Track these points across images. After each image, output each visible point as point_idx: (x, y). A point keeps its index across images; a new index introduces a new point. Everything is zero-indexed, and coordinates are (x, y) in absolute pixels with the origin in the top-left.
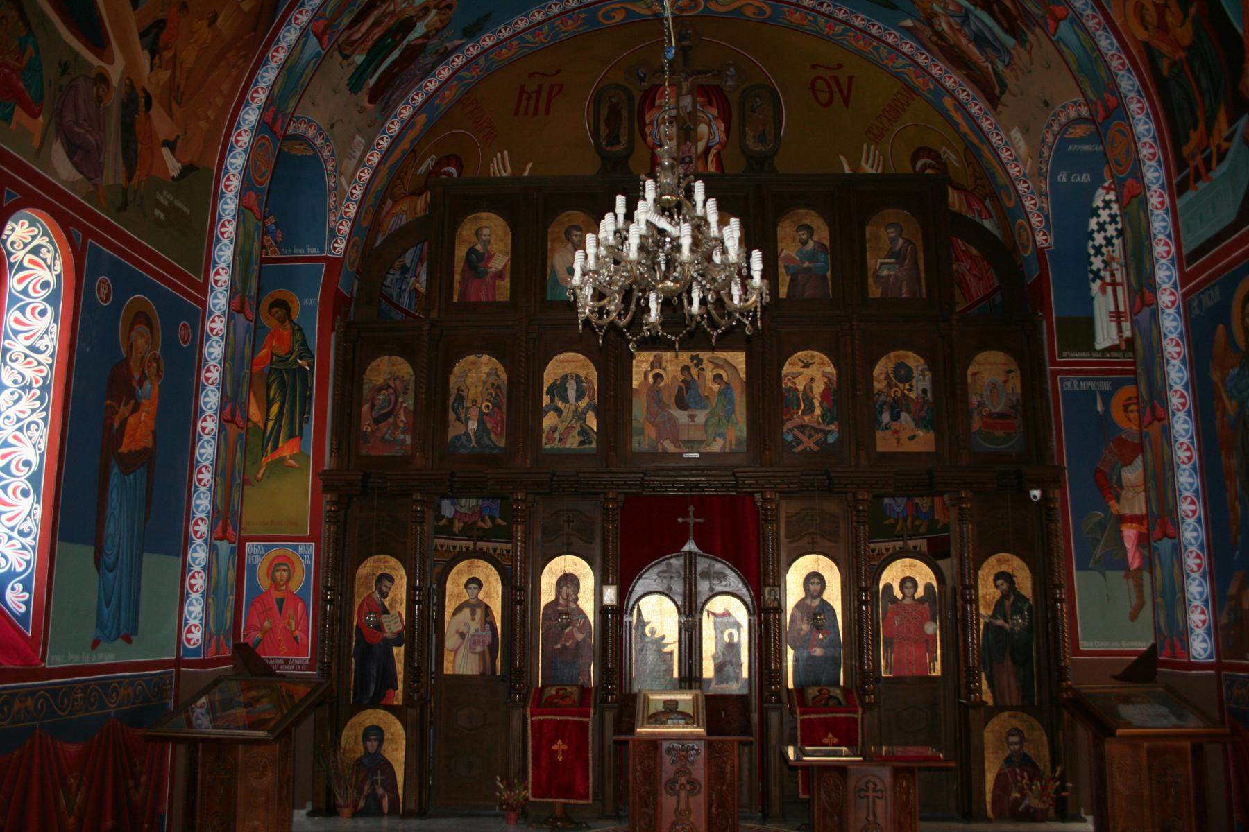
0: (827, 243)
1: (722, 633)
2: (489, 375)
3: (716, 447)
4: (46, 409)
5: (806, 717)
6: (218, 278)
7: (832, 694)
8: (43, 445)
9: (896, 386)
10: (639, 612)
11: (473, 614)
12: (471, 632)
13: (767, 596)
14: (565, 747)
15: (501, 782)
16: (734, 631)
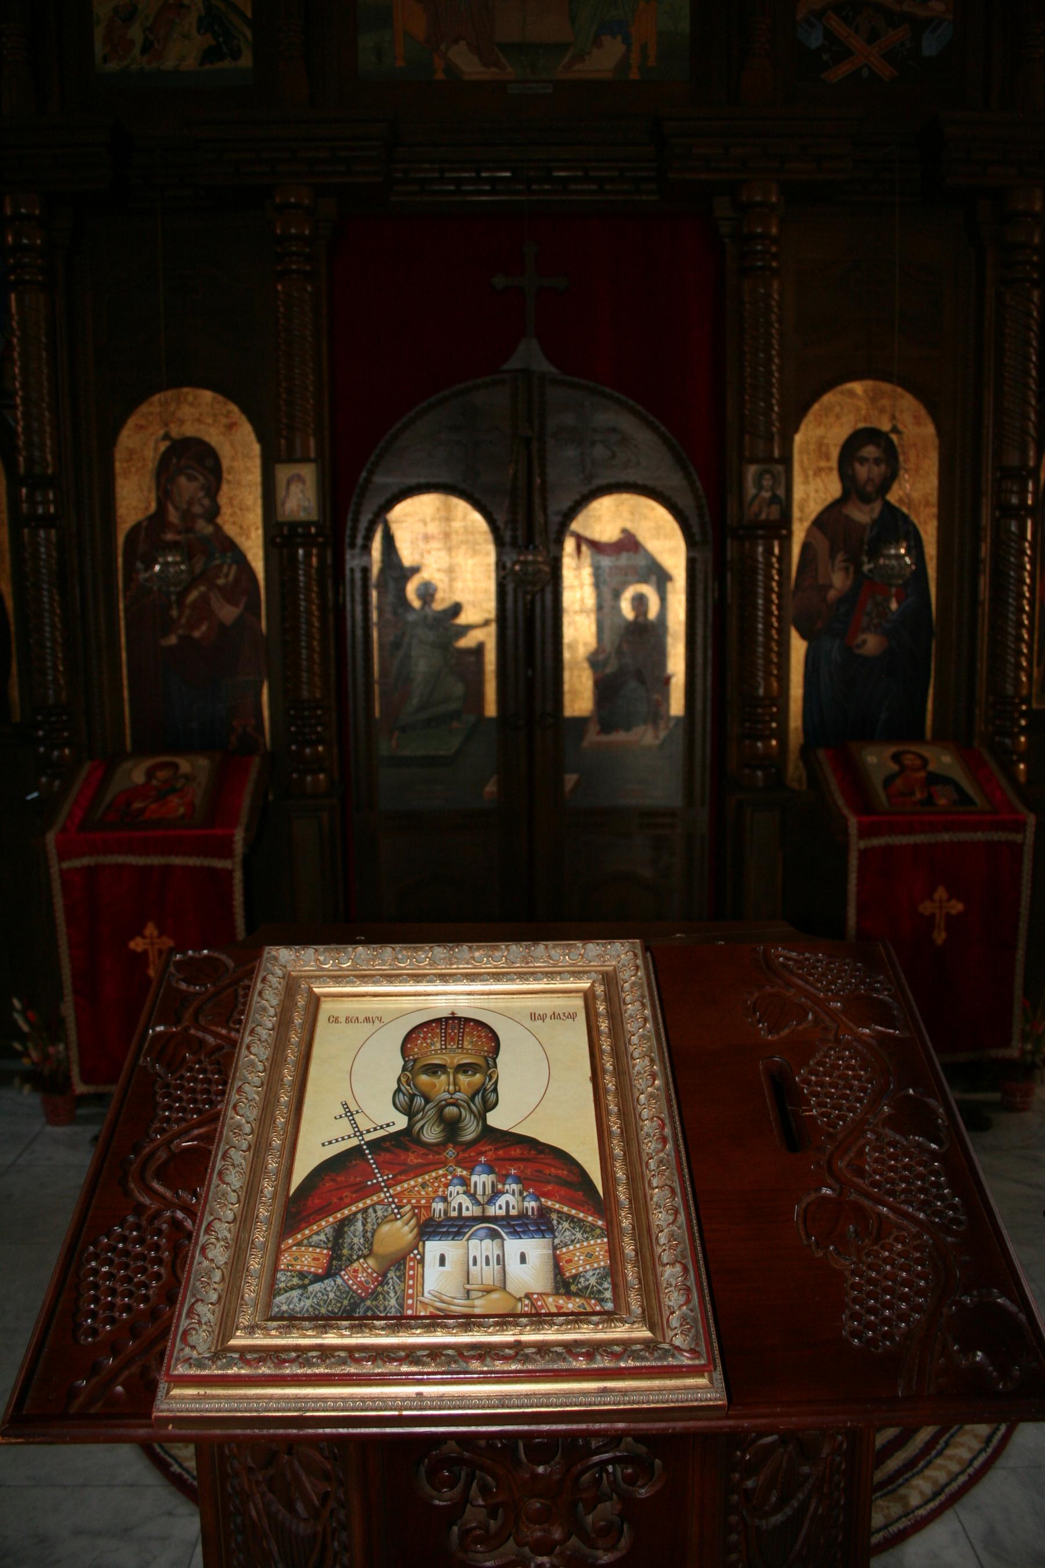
1: (617, 595)
5: (876, 842)
7: (932, 767)
13: (751, 490)
16: (649, 591)
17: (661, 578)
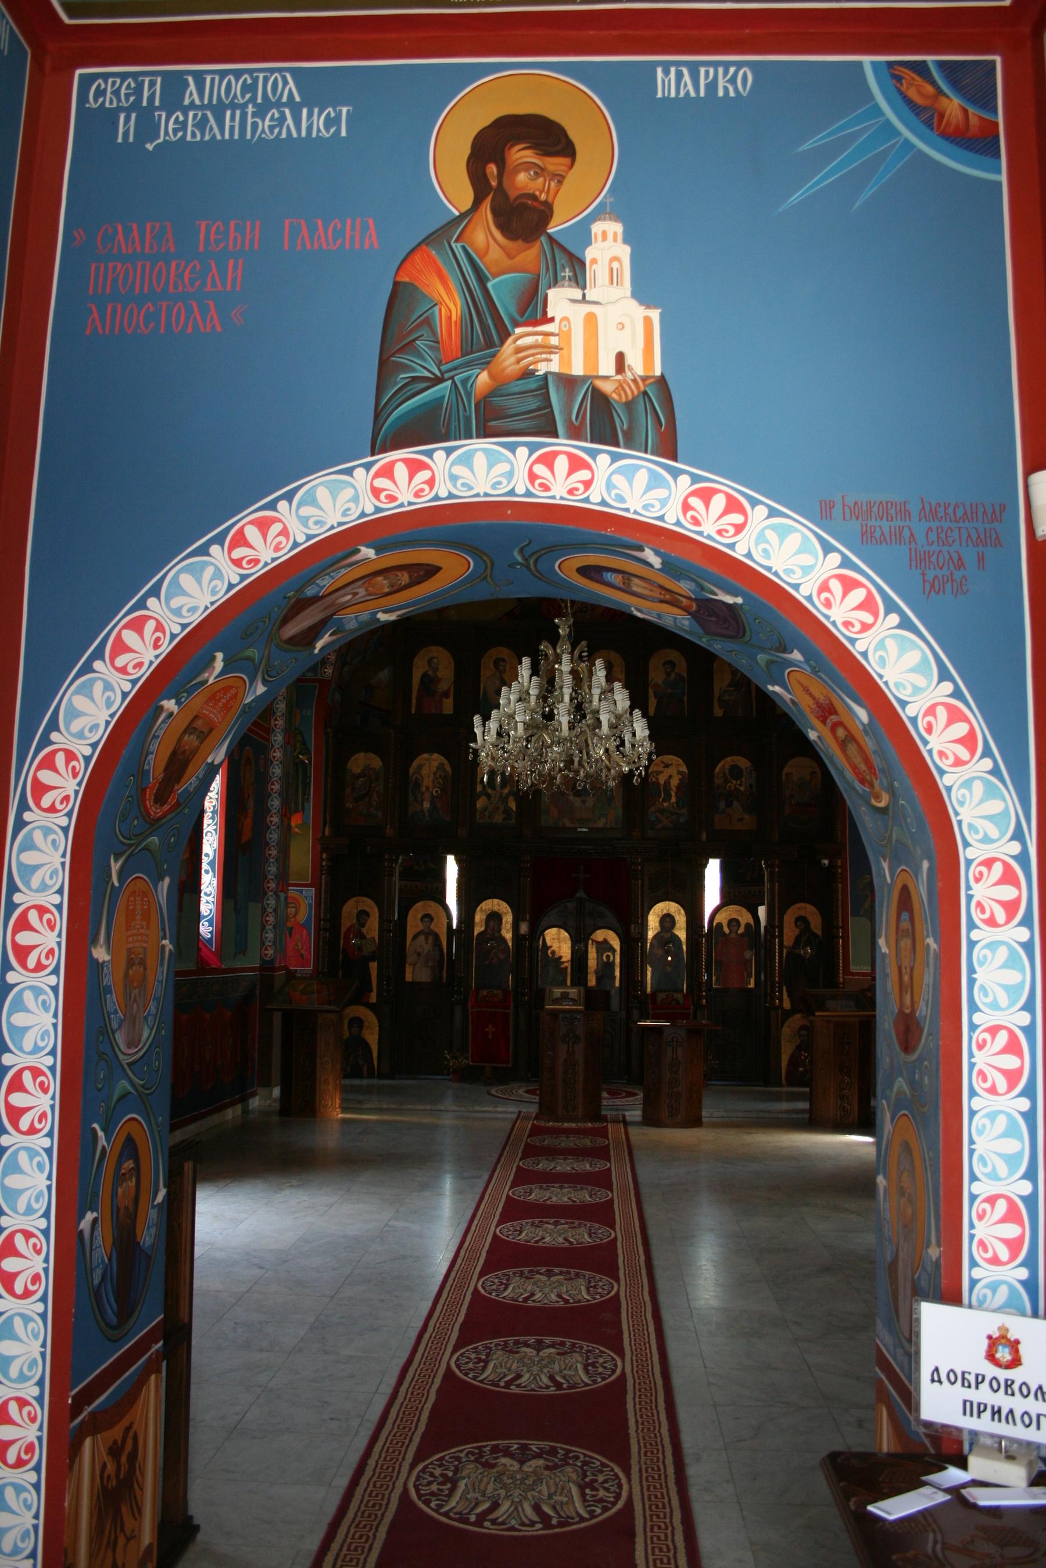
0: (685, 675)
1: (602, 956)
2: (438, 768)
3: (601, 823)
4: (216, 824)
6: (276, 722)
8: (216, 845)
9: (731, 782)
10: (544, 940)
11: (427, 939)
12: (426, 951)
13: (632, 930)
14: (494, 1030)
15: (449, 1054)
17: (614, 951)
